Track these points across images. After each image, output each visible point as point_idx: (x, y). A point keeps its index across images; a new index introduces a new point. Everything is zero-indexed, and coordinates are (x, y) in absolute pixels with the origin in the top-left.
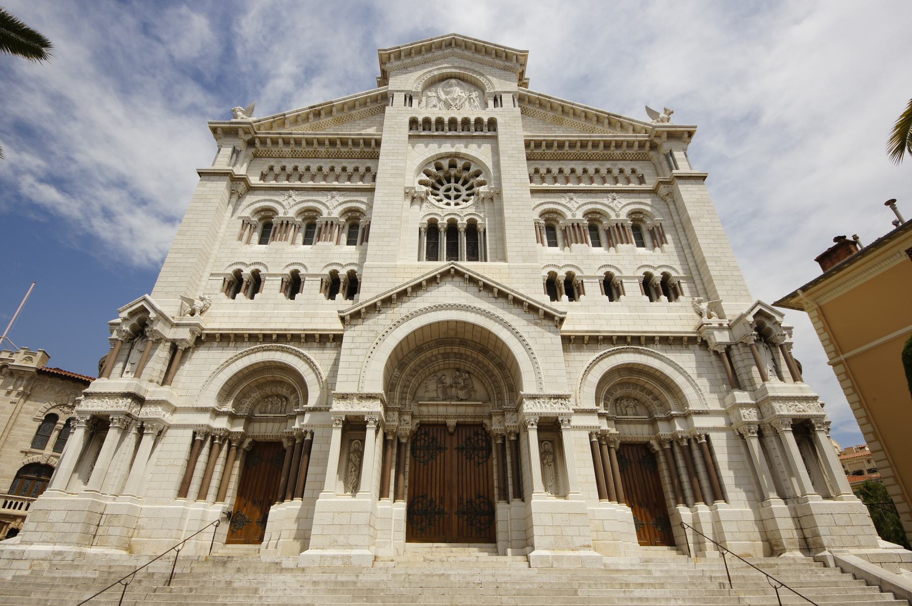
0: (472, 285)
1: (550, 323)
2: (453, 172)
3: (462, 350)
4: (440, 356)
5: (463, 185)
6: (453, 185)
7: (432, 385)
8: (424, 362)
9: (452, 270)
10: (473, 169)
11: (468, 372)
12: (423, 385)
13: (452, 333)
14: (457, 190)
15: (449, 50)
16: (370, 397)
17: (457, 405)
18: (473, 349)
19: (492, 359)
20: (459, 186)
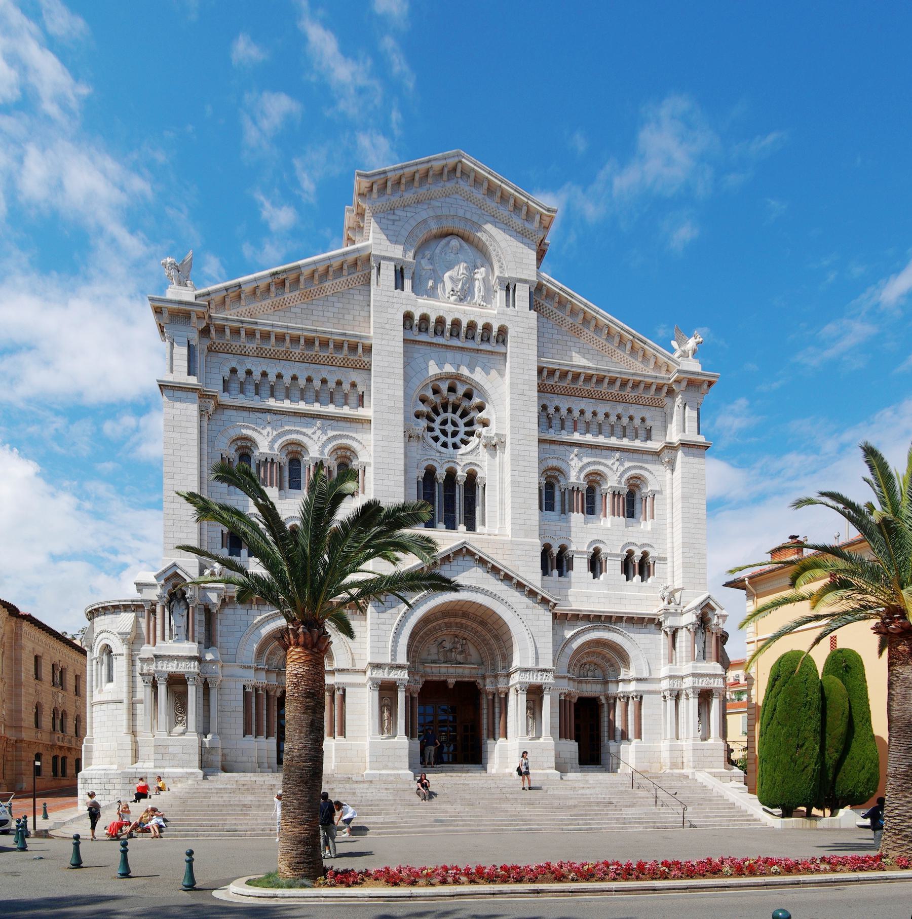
0: (481, 565)
1: (546, 607)
3: (464, 621)
4: (442, 625)
7: (434, 650)
8: (429, 630)
9: (464, 550)
11: (465, 639)
12: (426, 648)
13: (457, 608)
16: (400, 667)
17: (456, 667)
18: (474, 621)
19: (490, 631)
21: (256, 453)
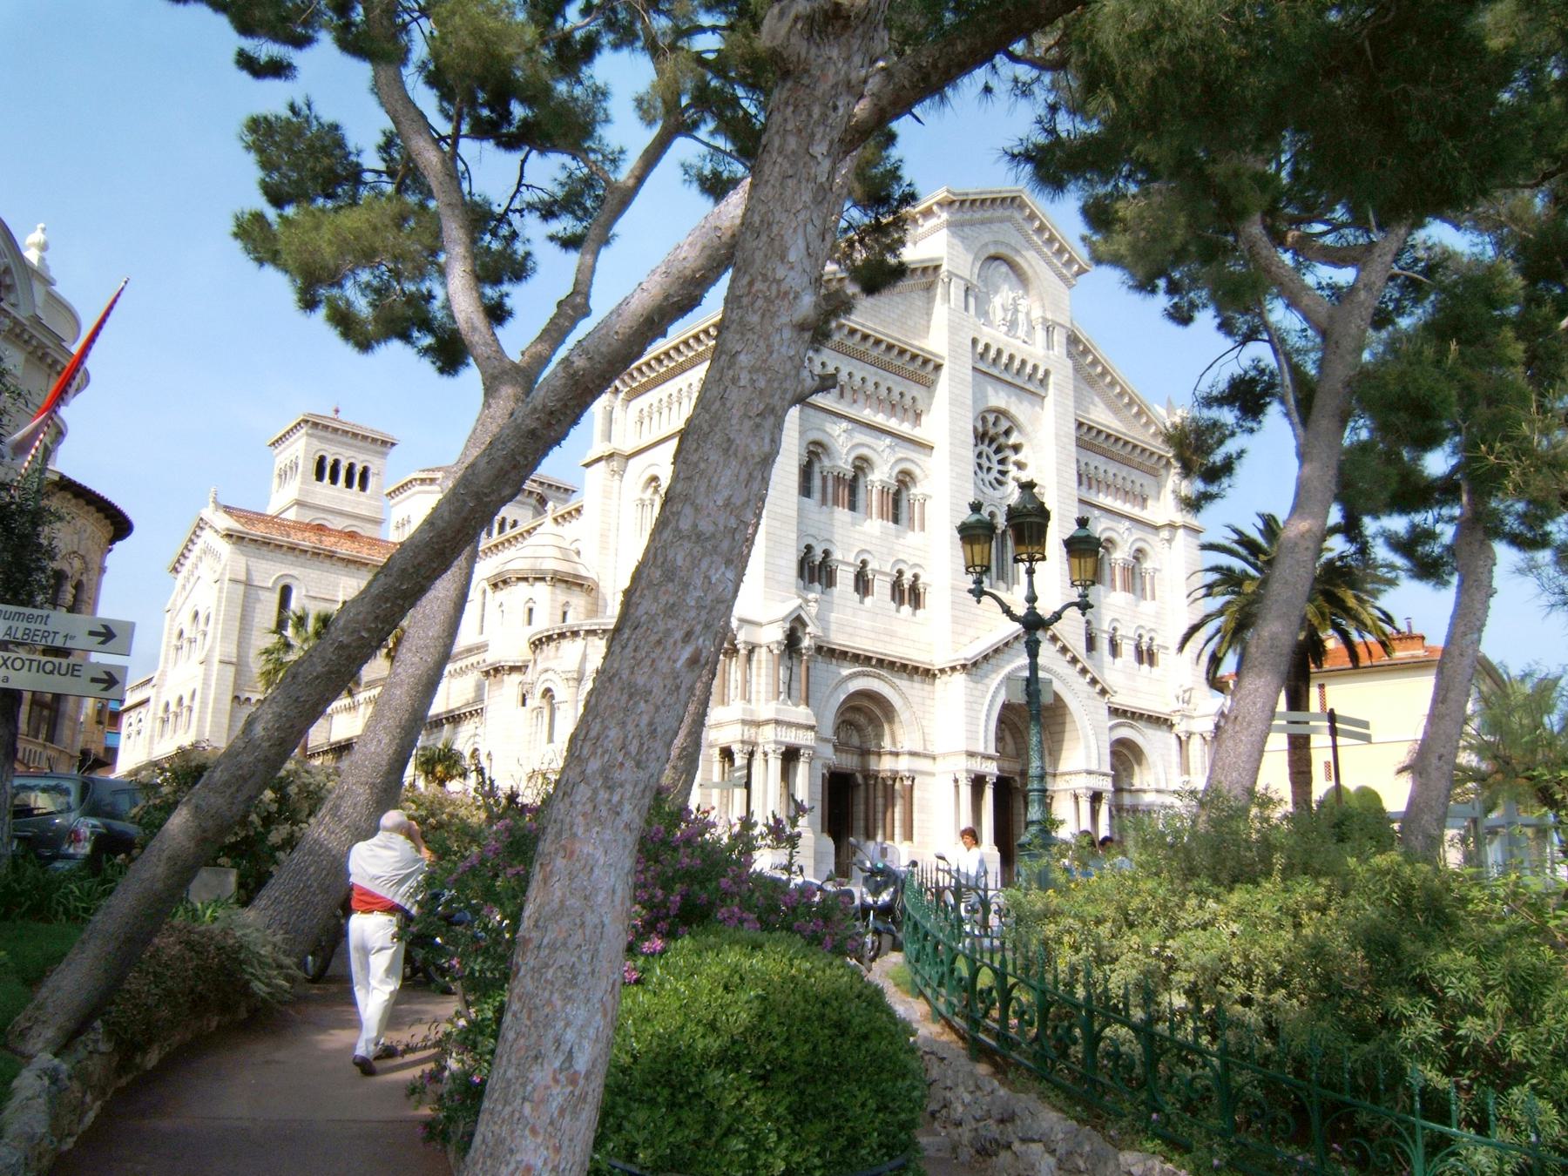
2: (992, 432)
5: (997, 451)
6: (984, 448)
10: (1013, 440)
14: (988, 458)
15: (1008, 213)
16: (989, 758)
20: (991, 451)
21: (826, 462)
